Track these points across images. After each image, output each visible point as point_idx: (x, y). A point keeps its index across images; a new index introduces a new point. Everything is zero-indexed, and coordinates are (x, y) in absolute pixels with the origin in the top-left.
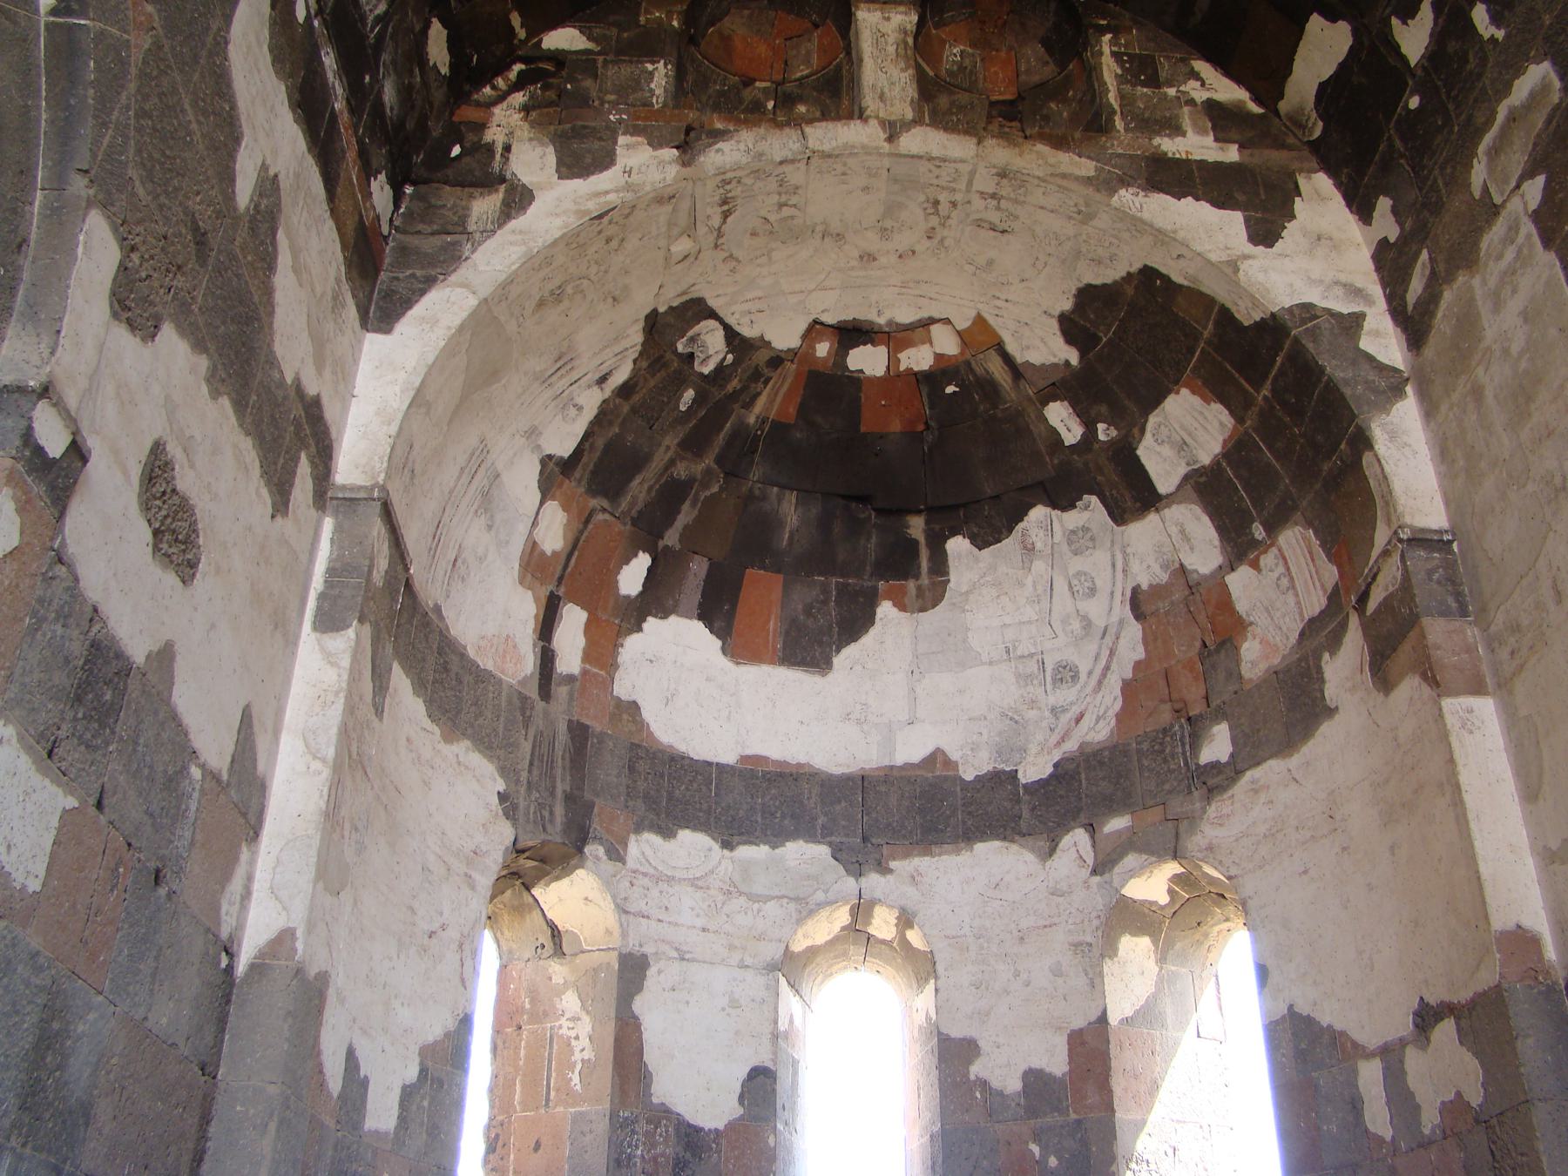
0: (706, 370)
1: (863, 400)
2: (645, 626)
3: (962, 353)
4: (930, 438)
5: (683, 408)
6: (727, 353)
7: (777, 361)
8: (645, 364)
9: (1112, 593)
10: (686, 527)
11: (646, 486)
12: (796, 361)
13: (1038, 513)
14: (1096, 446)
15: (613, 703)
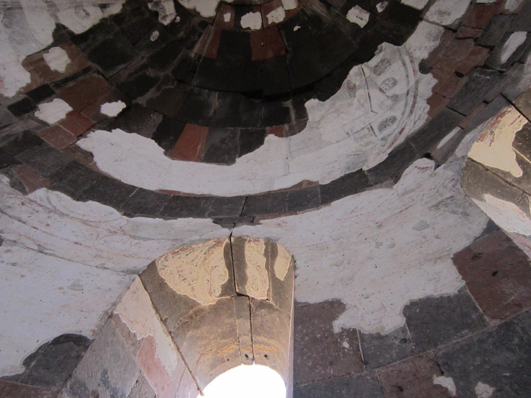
0: (166, 22)
1: (251, 44)
2: (113, 131)
3: (298, 6)
4: (289, 56)
5: (152, 39)
6: (177, 16)
7: (205, 23)
8: (129, 9)
9: (407, 76)
10: (151, 99)
11: (128, 72)
12: (214, 25)
13: (355, 70)
14: (378, 18)
15: (73, 146)
